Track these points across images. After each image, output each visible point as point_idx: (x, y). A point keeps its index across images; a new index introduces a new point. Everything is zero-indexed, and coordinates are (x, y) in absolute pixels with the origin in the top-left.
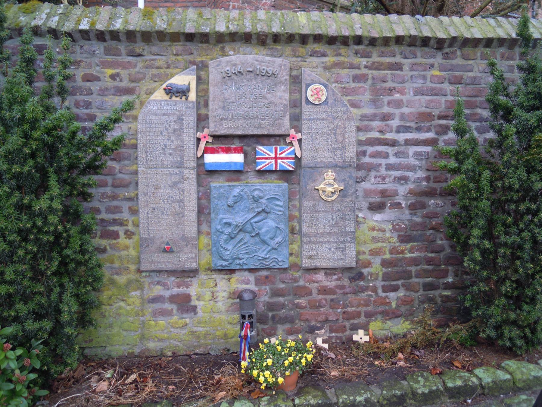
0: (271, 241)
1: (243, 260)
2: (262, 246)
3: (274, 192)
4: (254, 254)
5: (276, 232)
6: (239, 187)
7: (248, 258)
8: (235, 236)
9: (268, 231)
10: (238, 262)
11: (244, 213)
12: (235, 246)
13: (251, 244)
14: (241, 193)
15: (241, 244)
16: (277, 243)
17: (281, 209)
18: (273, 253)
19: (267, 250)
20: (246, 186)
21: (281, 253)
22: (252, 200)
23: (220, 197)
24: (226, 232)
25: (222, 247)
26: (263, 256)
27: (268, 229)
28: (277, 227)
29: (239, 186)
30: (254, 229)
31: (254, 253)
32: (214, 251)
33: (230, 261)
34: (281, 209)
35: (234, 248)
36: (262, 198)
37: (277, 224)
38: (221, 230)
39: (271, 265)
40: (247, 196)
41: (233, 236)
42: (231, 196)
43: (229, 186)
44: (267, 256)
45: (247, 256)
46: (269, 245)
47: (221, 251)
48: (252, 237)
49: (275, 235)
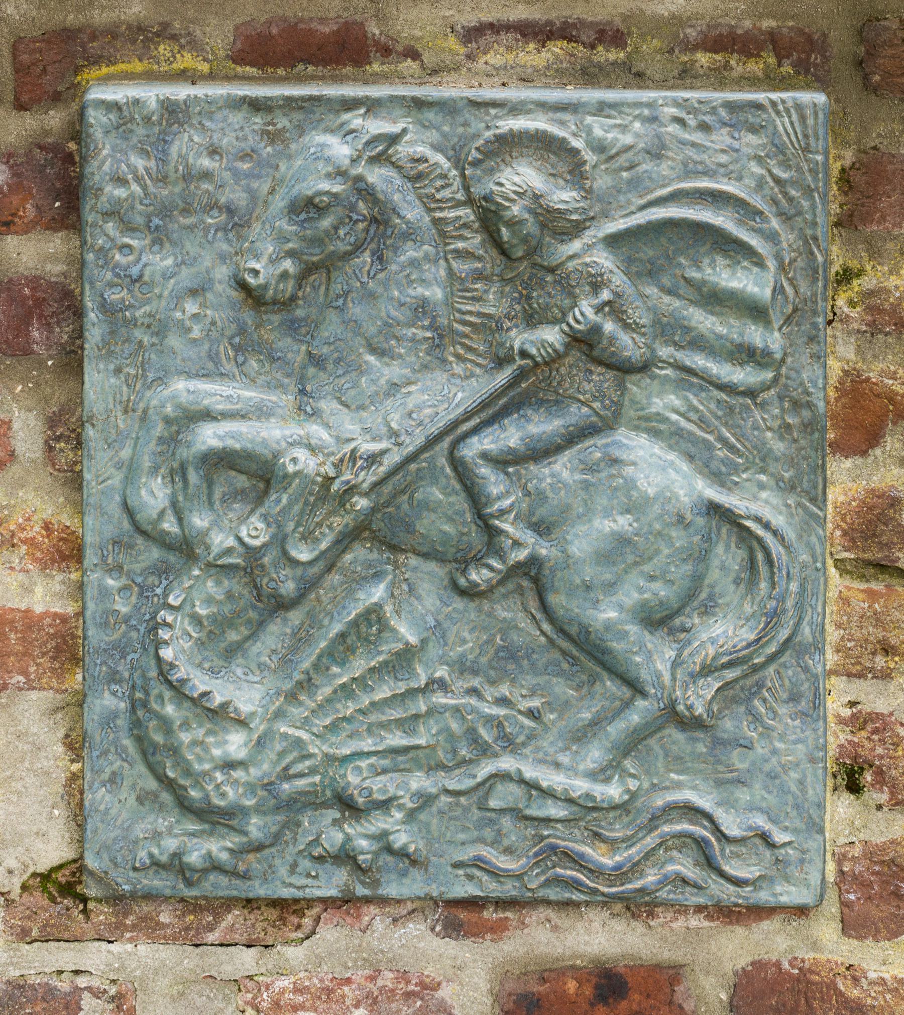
0: (651, 641)
1: (378, 823)
2: (563, 689)
3: (689, 172)
4: (485, 769)
5: (702, 557)
6: (355, 120)
7: (425, 800)
8: (308, 587)
9: (622, 541)
10: (333, 839)
11: (393, 371)
12: (307, 684)
13: (463, 667)
14: (376, 176)
15: (359, 665)
16: (707, 670)
17: (755, 335)
18: (677, 762)
19: (616, 729)
20: (419, 104)
21: (739, 761)
22: (474, 241)
23: (166, 211)
24: (220, 540)
25: (178, 690)
26: (580, 786)
27: (623, 523)
28: (714, 509)
29: (350, 105)
30: (491, 533)
31: (484, 751)
32: (110, 719)
33: (256, 826)
34: (755, 335)
35: (292, 697)
36: (577, 229)
37: (718, 478)
38: (169, 525)
39: (651, 878)
40: (429, 203)
41: (289, 588)
42: (279, 203)
43: (256, 105)
44: (614, 791)
45: (418, 781)
46: (637, 688)
47: (166, 725)
48: (470, 593)
49: (697, 579)
